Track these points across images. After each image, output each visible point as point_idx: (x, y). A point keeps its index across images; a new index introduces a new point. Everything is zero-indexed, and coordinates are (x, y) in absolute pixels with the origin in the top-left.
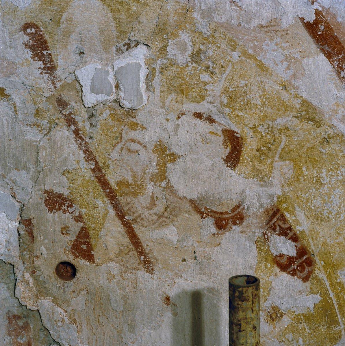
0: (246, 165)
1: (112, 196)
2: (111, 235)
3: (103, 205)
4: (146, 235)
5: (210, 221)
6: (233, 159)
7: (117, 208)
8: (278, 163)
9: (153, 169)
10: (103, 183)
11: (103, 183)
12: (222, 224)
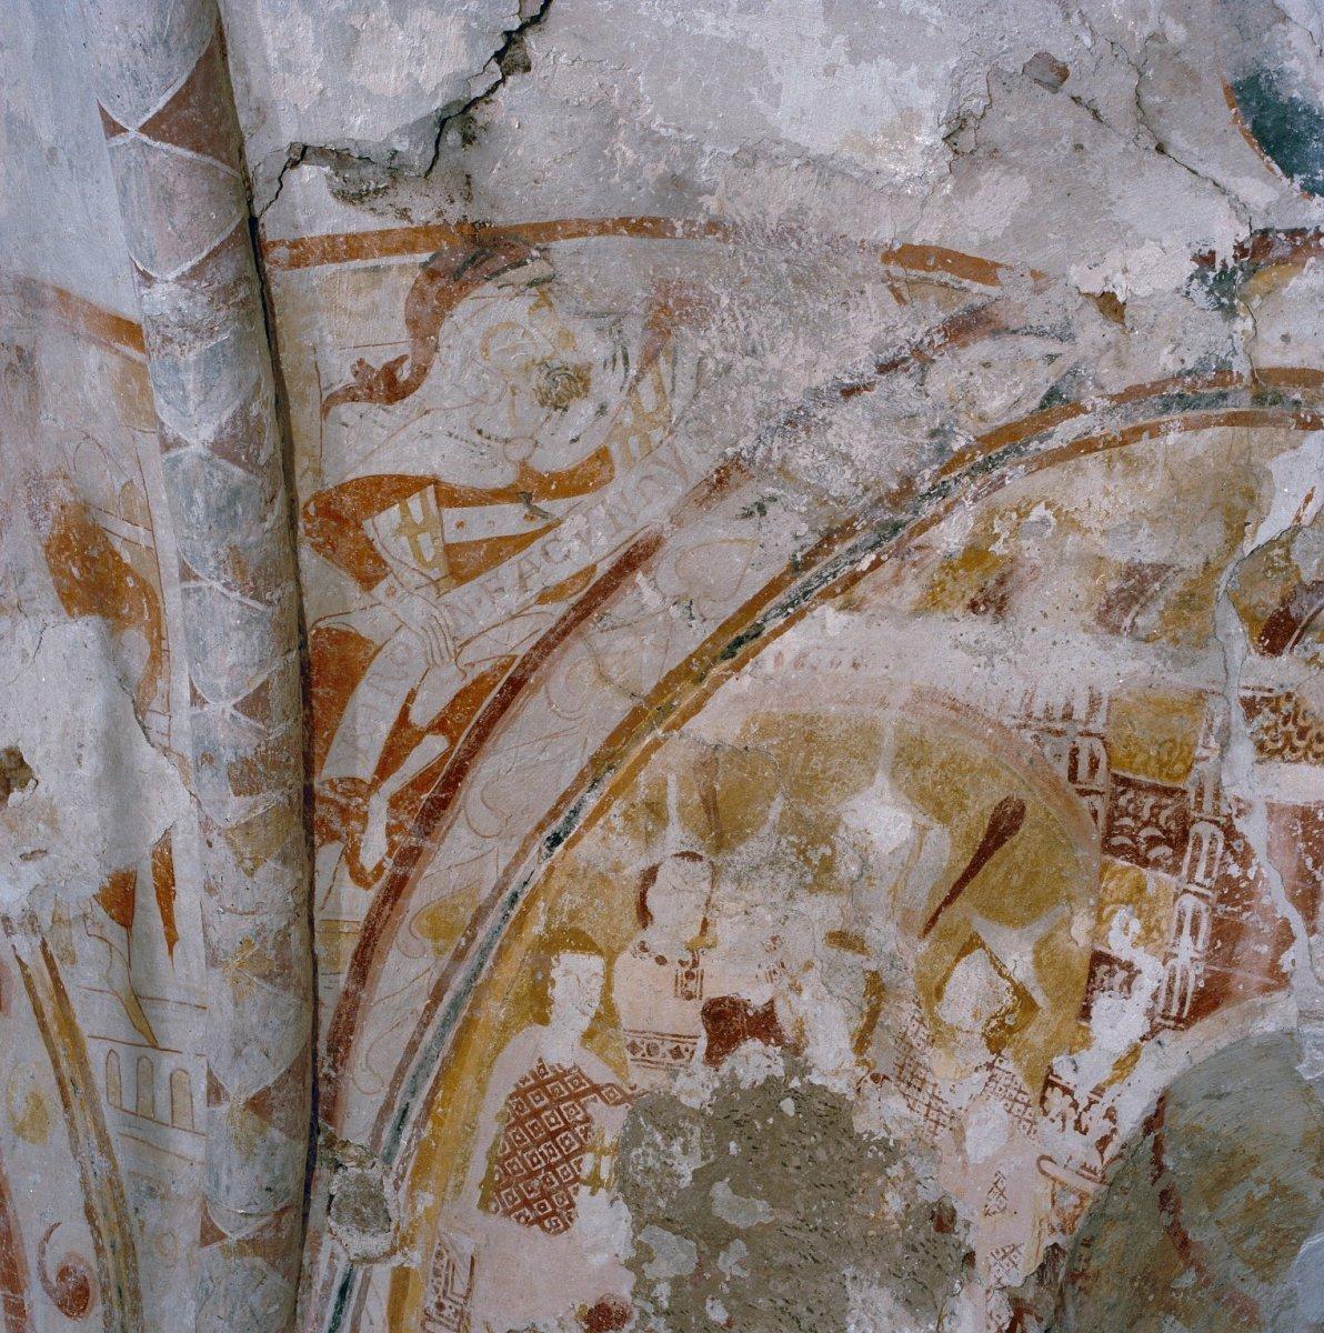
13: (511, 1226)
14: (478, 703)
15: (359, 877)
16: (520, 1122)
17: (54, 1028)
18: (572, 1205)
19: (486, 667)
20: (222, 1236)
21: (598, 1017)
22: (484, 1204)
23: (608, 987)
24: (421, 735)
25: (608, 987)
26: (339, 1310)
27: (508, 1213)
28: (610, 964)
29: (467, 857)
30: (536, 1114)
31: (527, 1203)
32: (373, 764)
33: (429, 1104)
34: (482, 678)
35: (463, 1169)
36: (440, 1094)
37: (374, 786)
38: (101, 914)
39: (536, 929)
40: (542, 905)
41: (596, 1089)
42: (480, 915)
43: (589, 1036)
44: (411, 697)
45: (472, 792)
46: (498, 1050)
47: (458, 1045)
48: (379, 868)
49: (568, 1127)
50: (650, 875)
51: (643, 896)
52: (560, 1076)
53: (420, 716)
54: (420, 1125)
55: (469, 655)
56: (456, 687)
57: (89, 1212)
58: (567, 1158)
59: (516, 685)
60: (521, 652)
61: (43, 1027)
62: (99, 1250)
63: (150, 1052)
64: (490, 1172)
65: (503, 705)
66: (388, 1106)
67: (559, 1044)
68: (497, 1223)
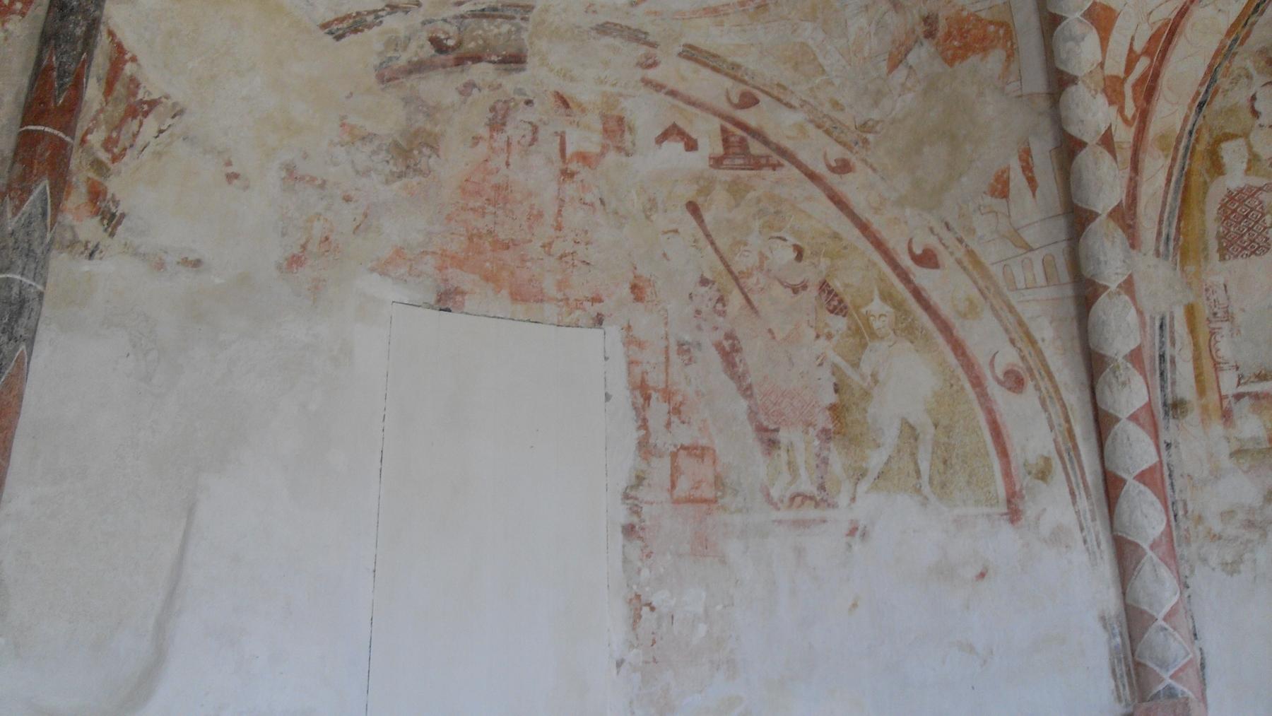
0: (806, 262)
1: (736, 279)
2: (736, 300)
3: (731, 285)
4: (754, 298)
5: (790, 291)
6: (799, 257)
7: (738, 284)
8: (822, 260)
9: (757, 264)
10: (731, 272)
11: (731, 272)
12: (795, 291)
13: (1240, 261)
14: (1158, 41)
15: (1125, 121)
16: (1227, 218)
17: (970, 267)
18: (1267, 239)
19: (1159, 24)
20: (1106, 288)
21: (1249, 161)
22: (1223, 258)
23: (1250, 147)
24: (1137, 59)
25: (1250, 147)
26: (1162, 336)
27: (1236, 257)
28: (1246, 135)
29: (1170, 112)
30: (1234, 211)
31: (1245, 248)
32: (1123, 67)
33: (1178, 229)
34: (1159, 29)
35: (1205, 249)
36: (1182, 224)
37: (1124, 80)
38: (988, 200)
39: (1206, 138)
40: (1204, 130)
41: (1260, 189)
42: (1179, 141)
43: (1248, 169)
44: (1133, 39)
45: (1164, 81)
46: (1205, 193)
47: (1184, 200)
48: (1134, 117)
49: (1252, 209)
50: (1254, 98)
51: (1253, 107)
52: (1240, 191)
53: (1138, 47)
54: (1177, 239)
55: (1151, 20)
56: (1150, 33)
57: (1012, 342)
58: (1257, 222)
59: (1172, 33)
60: (1172, 17)
61: (964, 269)
62: (1023, 358)
63: (1029, 255)
64: (1220, 244)
65: (1169, 41)
66: (1159, 233)
67: (1235, 178)
68: (1230, 263)
